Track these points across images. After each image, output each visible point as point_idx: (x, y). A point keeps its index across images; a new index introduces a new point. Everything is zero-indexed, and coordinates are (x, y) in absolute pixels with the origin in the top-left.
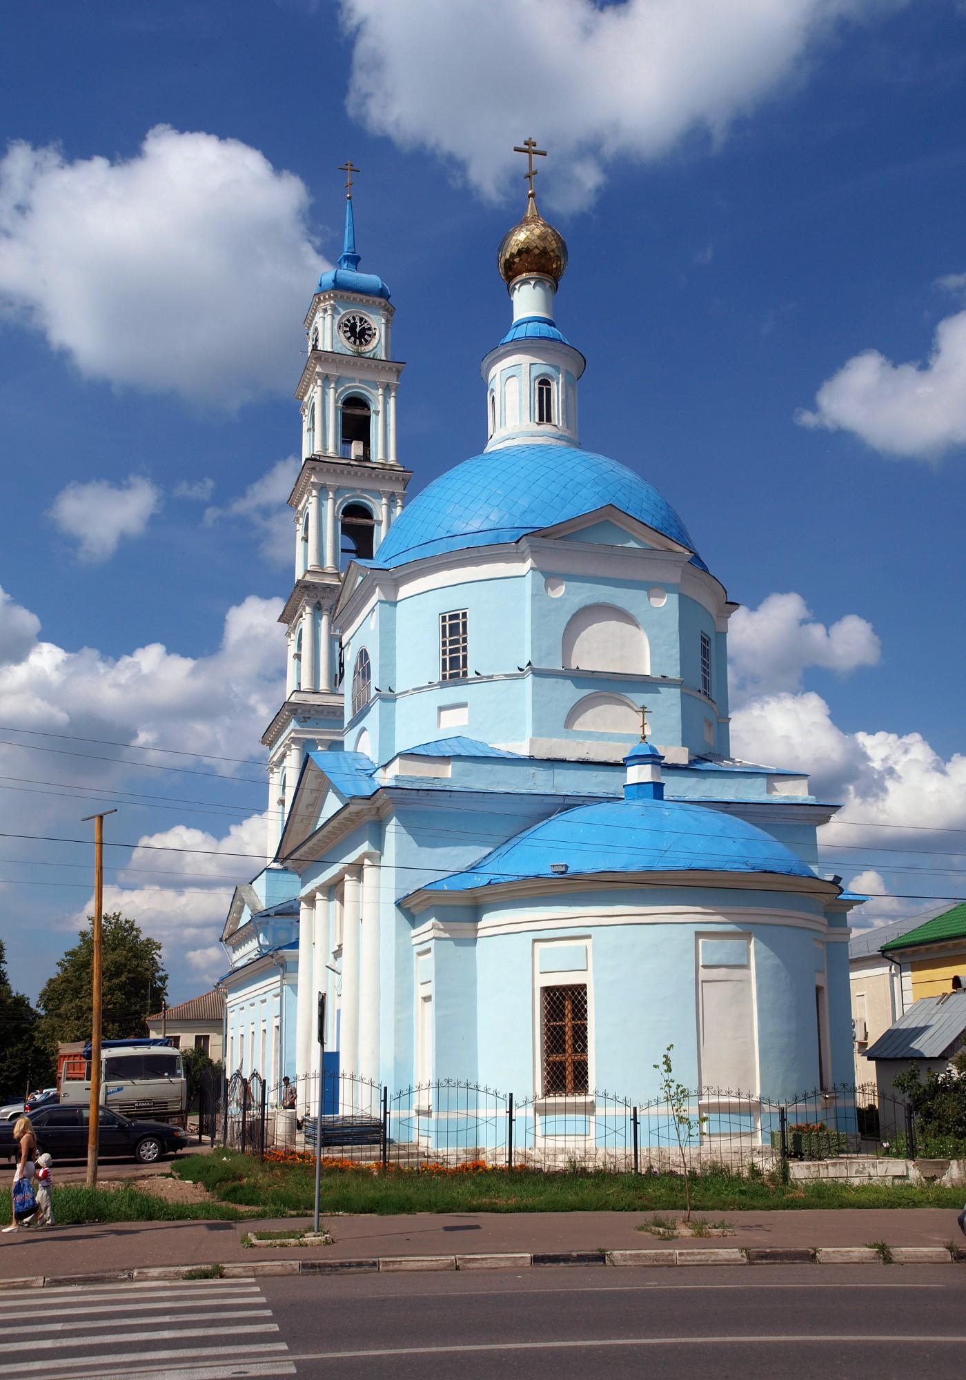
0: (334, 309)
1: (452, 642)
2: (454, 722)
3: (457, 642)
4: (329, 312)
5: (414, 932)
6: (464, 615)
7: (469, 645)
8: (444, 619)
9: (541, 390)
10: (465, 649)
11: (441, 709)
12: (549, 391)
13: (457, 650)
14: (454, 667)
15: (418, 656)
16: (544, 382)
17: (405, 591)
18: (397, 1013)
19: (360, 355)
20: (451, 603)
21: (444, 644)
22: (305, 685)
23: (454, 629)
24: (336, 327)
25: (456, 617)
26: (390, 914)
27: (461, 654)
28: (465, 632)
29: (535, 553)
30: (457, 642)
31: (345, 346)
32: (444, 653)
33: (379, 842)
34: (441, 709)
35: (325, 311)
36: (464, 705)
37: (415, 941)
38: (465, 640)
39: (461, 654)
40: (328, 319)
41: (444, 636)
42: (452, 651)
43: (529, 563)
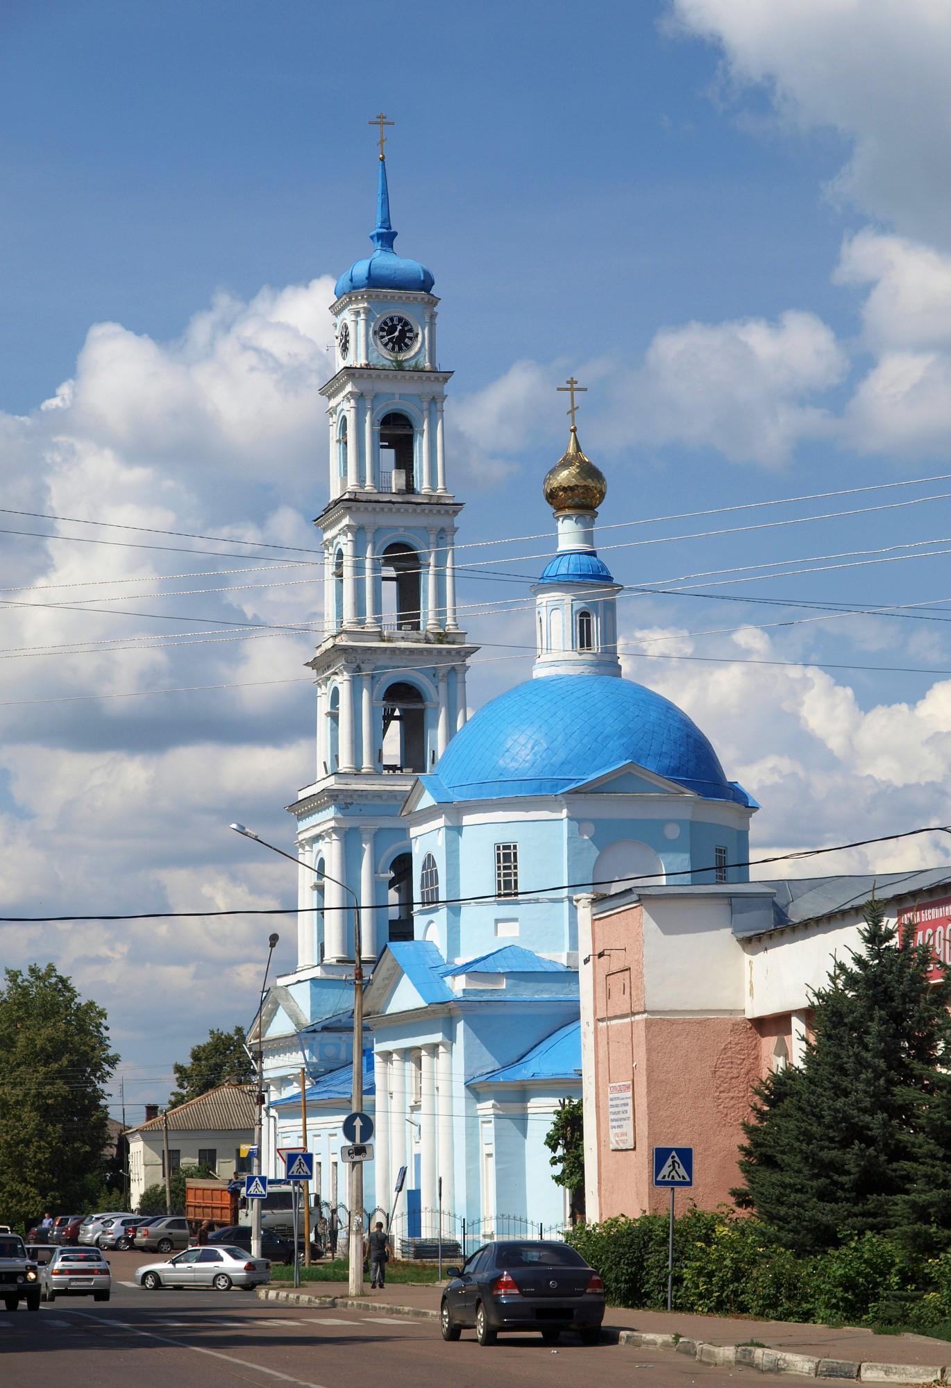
0: (368, 311)
1: (505, 868)
2: (509, 934)
3: (509, 867)
4: (363, 316)
5: (479, 1106)
6: (515, 847)
7: (519, 871)
8: (498, 848)
9: (581, 621)
10: (516, 874)
11: (497, 921)
12: (589, 622)
13: (509, 875)
14: (508, 889)
15: (478, 875)
16: (584, 614)
17: (467, 820)
18: (467, 1164)
19: (400, 366)
20: (506, 836)
21: (499, 868)
22: (345, 764)
23: (507, 857)
24: (371, 333)
25: (507, 847)
26: (460, 1090)
27: (513, 878)
28: (515, 860)
29: (569, 806)
30: (509, 867)
31: (384, 357)
32: (499, 875)
33: (451, 1036)
34: (497, 921)
35: (357, 314)
36: (515, 920)
37: (480, 1112)
38: (516, 867)
39: (513, 878)
40: (362, 324)
41: (499, 862)
42: (505, 875)
43: (564, 813)
